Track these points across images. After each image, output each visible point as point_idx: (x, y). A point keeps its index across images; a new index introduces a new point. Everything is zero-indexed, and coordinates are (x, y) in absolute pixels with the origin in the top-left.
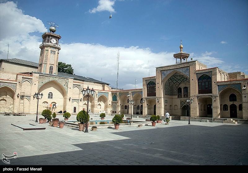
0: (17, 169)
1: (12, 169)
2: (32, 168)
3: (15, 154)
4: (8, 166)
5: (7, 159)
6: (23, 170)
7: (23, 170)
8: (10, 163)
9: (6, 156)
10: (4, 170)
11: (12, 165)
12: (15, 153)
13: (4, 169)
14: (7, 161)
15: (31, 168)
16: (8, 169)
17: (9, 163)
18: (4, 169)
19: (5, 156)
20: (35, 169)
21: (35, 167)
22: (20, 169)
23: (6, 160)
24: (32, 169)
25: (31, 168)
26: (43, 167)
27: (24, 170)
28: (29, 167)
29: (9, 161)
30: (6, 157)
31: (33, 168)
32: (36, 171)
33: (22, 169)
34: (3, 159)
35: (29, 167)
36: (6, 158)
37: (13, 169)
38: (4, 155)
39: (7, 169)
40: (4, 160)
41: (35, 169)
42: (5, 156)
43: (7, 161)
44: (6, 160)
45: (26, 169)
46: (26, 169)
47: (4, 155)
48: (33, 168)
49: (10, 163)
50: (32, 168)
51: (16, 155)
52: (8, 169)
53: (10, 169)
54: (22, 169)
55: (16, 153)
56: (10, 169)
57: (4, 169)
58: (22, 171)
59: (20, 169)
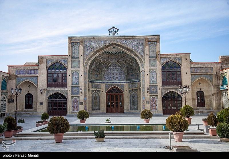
0: (16, 155)
1: (11, 156)
2: (29, 155)
6: (21, 156)
7: (21, 156)
9: (6, 143)
10: (3, 156)
13: (4, 156)
14: (7, 148)
15: (28, 154)
16: (8, 156)
18: (4, 156)
20: (32, 156)
22: (19, 156)
23: (6, 147)
25: (28, 154)
26: (40, 153)
27: (22, 156)
28: (27, 153)
29: (8, 148)
30: (5, 144)
31: (30, 154)
32: (34, 157)
33: (21, 156)
34: (3, 146)
36: (6, 145)
37: (12, 156)
38: (3, 142)
39: (7, 156)
40: (4, 147)
41: (32, 156)
43: (7, 148)
44: (6, 147)
45: (24, 156)
46: (24, 156)
48: (30, 154)
50: (29, 155)
52: (8, 156)
53: (9, 156)
54: (21, 156)
56: (9, 156)
57: (4, 156)
59: (19, 156)
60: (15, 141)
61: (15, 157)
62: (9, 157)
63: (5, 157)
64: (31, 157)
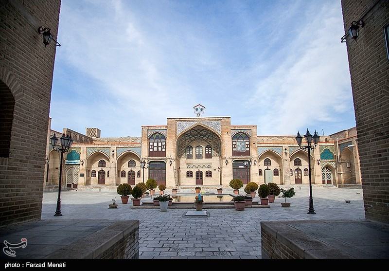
0: (27, 265)
1: (18, 265)
2: (50, 263)
3: (24, 242)
4: (13, 260)
5: (12, 249)
6: (36, 266)
7: (36, 266)
8: (15, 256)
10: (6, 267)
11: (19, 258)
12: (23, 240)
13: (7, 265)
14: (12, 253)
15: (48, 263)
16: (13, 265)
17: (14, 255)
18: (6, 265)
19: (8, 244)
20: (54, 265)
21: (54, 261)
22: (32, 265)
24: (50, 265)
25: (48, 263)
26: (67, 261)
27: (38, 266)
29: (14, 253)
30: (9, 245)
31: (51, 263)
32: (57, 268)
33: (35, 265)
34: (6, 249)
35: (46, 261)
37: (21, 265)
38: (6, 242)
39: (11, 265)
40: (6, 251)
41: (54, 265)
42: (8, 244)
43: (12, 253)
44: (10, 251)
45: (40, 265)
46: (40, 265)
47: (6, 242)
48: (51, 263)
49: (15, 256)
50: (50, 263)
51: (25, 243)
52: (13, 265)
53: (16, 265)
54: (35, 265)
55: (25, 240)
56: (16, 265)
57: (7, 265)
58: (34, 268)
59: (32, 265)
60: (25, 240)
61: (25, 268)
62: (15, 268)
63: (9, 268)
64: (52, 268)
